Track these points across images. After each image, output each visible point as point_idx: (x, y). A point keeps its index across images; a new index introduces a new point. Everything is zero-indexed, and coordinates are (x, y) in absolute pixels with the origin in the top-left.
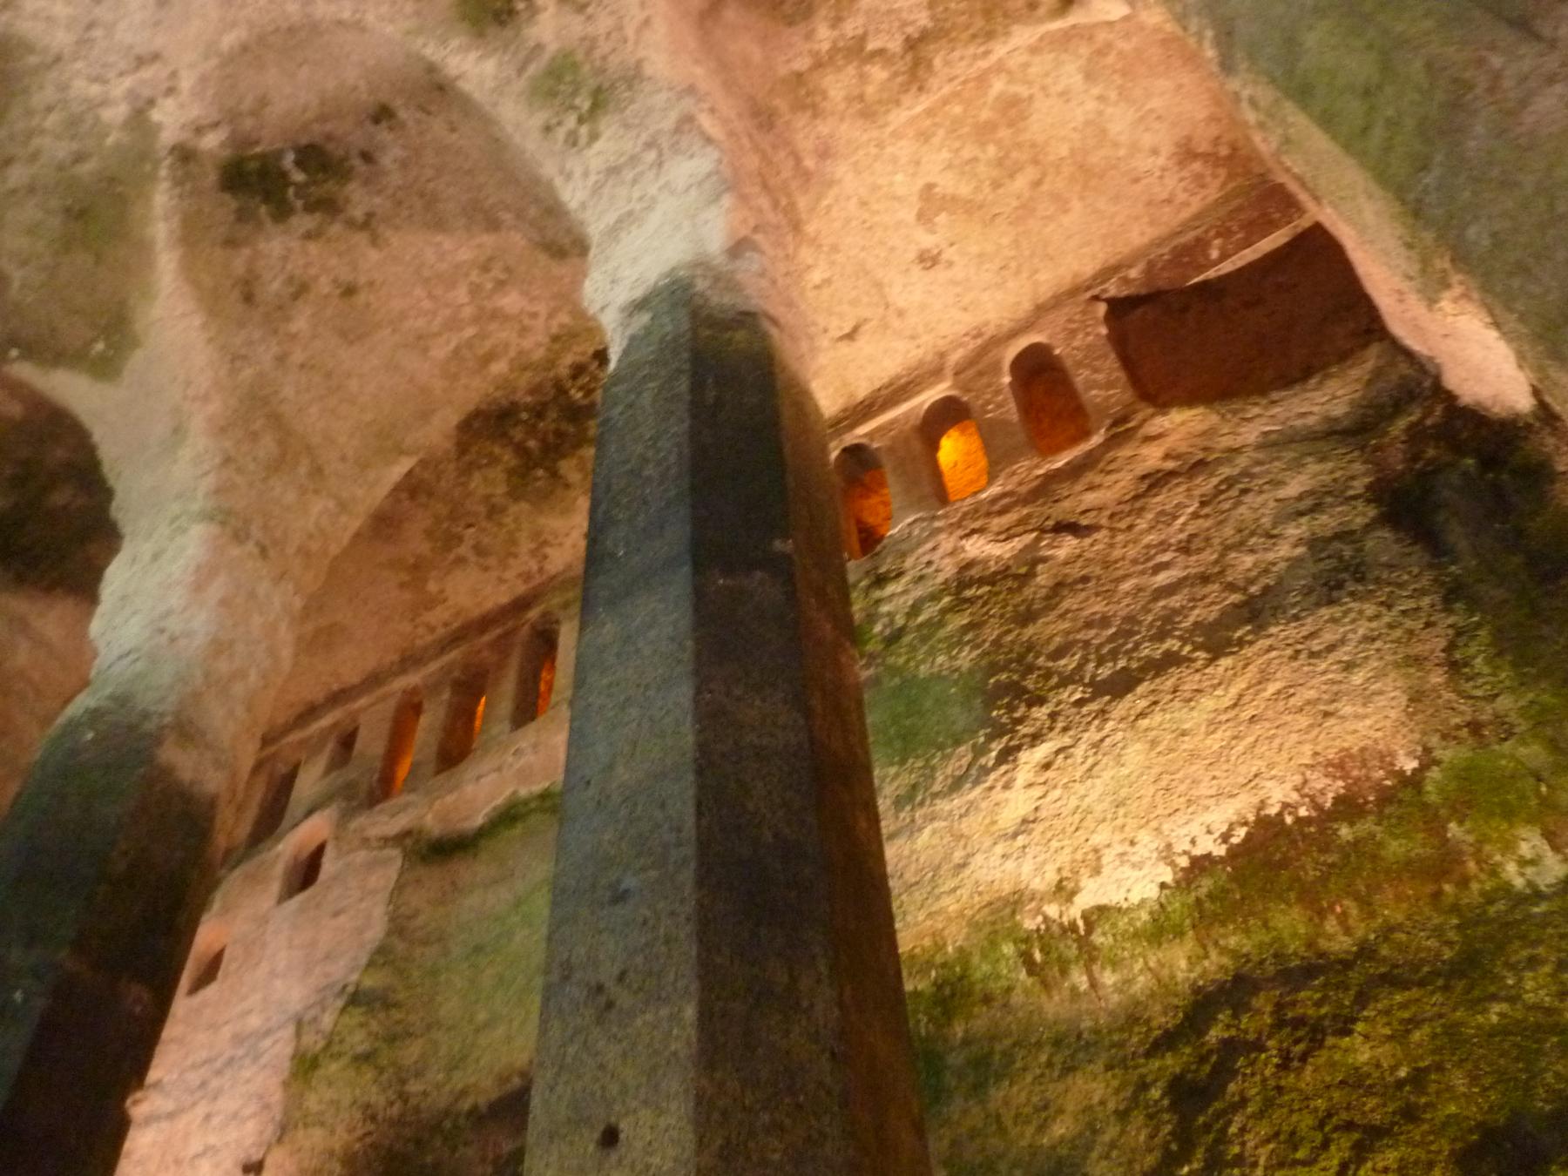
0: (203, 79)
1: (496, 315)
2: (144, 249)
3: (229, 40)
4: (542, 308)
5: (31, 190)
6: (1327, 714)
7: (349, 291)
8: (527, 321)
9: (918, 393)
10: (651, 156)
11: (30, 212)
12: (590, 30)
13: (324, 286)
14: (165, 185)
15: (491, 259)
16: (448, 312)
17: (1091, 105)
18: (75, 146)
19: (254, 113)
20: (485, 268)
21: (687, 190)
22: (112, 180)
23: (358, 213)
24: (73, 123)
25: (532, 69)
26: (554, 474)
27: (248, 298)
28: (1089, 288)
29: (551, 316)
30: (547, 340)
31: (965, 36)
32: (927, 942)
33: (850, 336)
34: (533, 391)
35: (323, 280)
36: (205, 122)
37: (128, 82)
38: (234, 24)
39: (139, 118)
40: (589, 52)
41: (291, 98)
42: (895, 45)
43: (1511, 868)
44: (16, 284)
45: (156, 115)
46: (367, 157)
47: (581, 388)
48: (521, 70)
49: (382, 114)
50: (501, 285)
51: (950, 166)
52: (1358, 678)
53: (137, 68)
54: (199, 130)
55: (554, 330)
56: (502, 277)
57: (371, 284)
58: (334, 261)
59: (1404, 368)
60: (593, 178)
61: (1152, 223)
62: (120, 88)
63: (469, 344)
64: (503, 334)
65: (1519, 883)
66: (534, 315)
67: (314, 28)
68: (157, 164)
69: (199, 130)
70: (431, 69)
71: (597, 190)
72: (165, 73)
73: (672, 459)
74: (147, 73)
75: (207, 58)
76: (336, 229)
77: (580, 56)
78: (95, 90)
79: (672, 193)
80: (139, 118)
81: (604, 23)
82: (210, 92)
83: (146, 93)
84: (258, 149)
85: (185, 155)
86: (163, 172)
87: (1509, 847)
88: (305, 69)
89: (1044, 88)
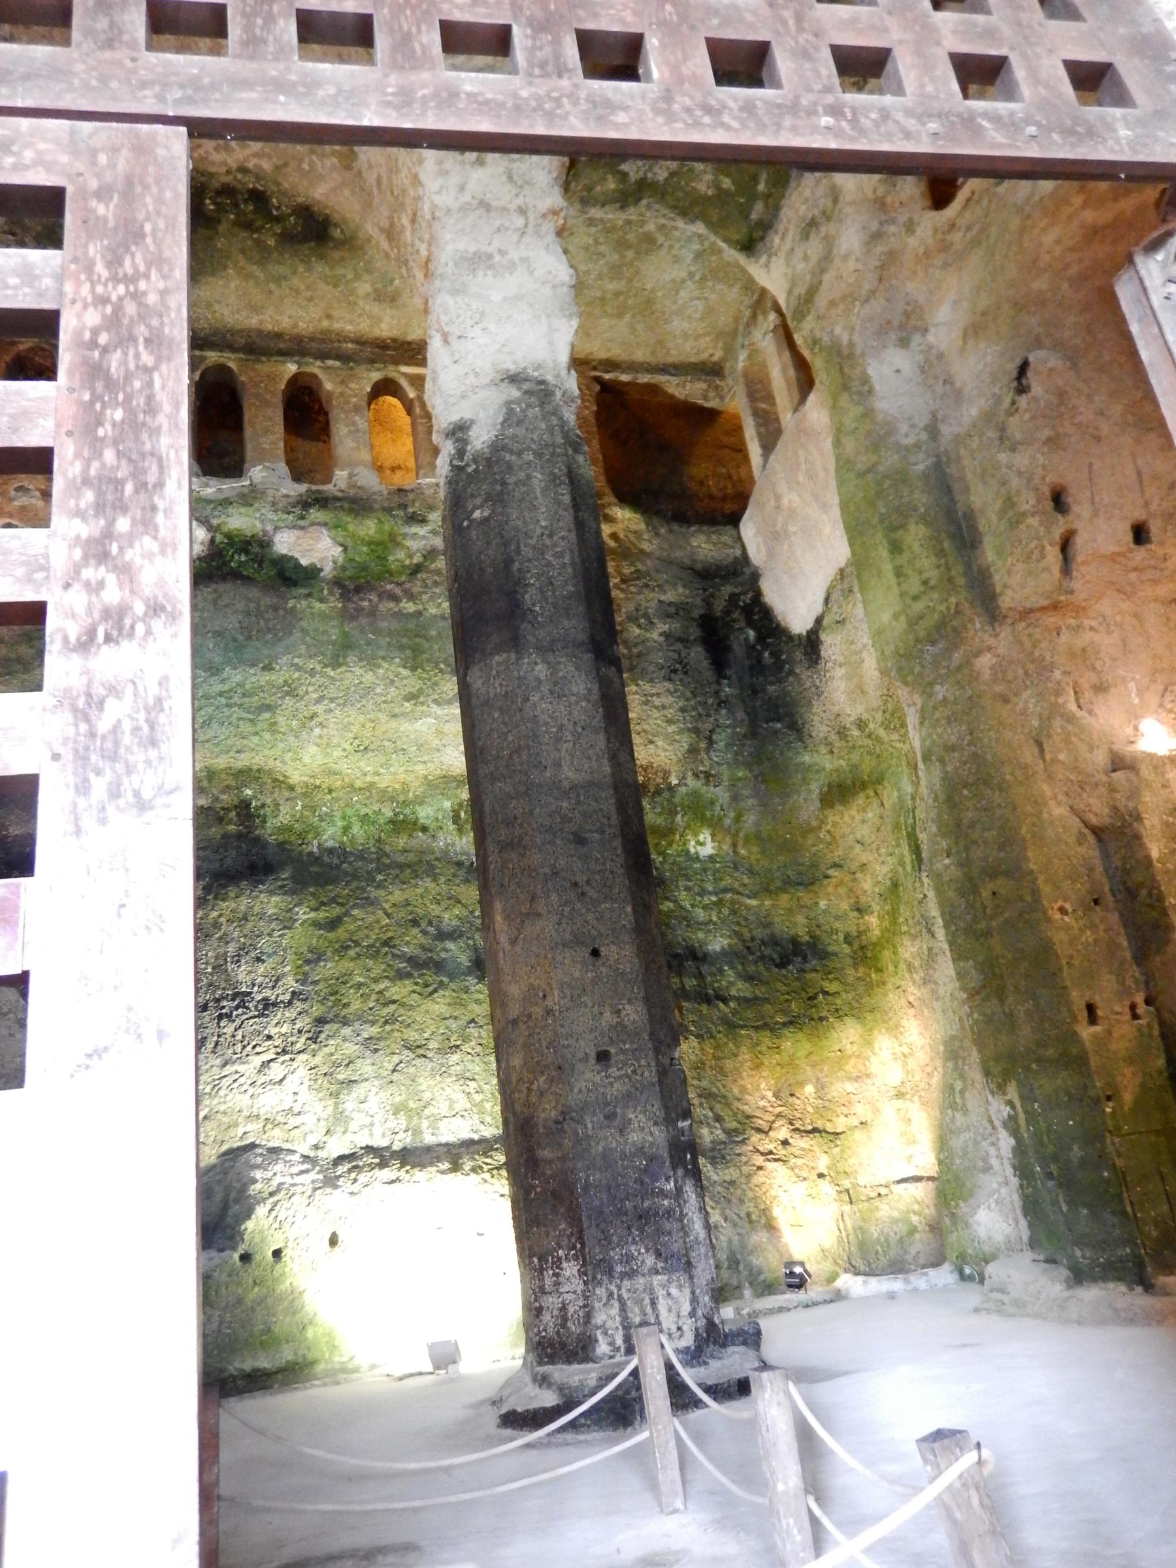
6: (651, 742)
10: (520, 222)
17: (684, 274)
21: (543, 283)
28: (595, 369)
31: (672, 203)
32: (397, 786)
42: (633, 177)
43: (693, 843)
47: (214, 203)
51: (587, 248)
52: (671, 729)
55: (250, 165)
59: (738, 552)
60: (466, 198)
61: (652, 353)
65: (692, 850)
71: (464, 209)
73: (567, 560)
79: (531, 273)
87: (696, 835)
89: (671, 247)
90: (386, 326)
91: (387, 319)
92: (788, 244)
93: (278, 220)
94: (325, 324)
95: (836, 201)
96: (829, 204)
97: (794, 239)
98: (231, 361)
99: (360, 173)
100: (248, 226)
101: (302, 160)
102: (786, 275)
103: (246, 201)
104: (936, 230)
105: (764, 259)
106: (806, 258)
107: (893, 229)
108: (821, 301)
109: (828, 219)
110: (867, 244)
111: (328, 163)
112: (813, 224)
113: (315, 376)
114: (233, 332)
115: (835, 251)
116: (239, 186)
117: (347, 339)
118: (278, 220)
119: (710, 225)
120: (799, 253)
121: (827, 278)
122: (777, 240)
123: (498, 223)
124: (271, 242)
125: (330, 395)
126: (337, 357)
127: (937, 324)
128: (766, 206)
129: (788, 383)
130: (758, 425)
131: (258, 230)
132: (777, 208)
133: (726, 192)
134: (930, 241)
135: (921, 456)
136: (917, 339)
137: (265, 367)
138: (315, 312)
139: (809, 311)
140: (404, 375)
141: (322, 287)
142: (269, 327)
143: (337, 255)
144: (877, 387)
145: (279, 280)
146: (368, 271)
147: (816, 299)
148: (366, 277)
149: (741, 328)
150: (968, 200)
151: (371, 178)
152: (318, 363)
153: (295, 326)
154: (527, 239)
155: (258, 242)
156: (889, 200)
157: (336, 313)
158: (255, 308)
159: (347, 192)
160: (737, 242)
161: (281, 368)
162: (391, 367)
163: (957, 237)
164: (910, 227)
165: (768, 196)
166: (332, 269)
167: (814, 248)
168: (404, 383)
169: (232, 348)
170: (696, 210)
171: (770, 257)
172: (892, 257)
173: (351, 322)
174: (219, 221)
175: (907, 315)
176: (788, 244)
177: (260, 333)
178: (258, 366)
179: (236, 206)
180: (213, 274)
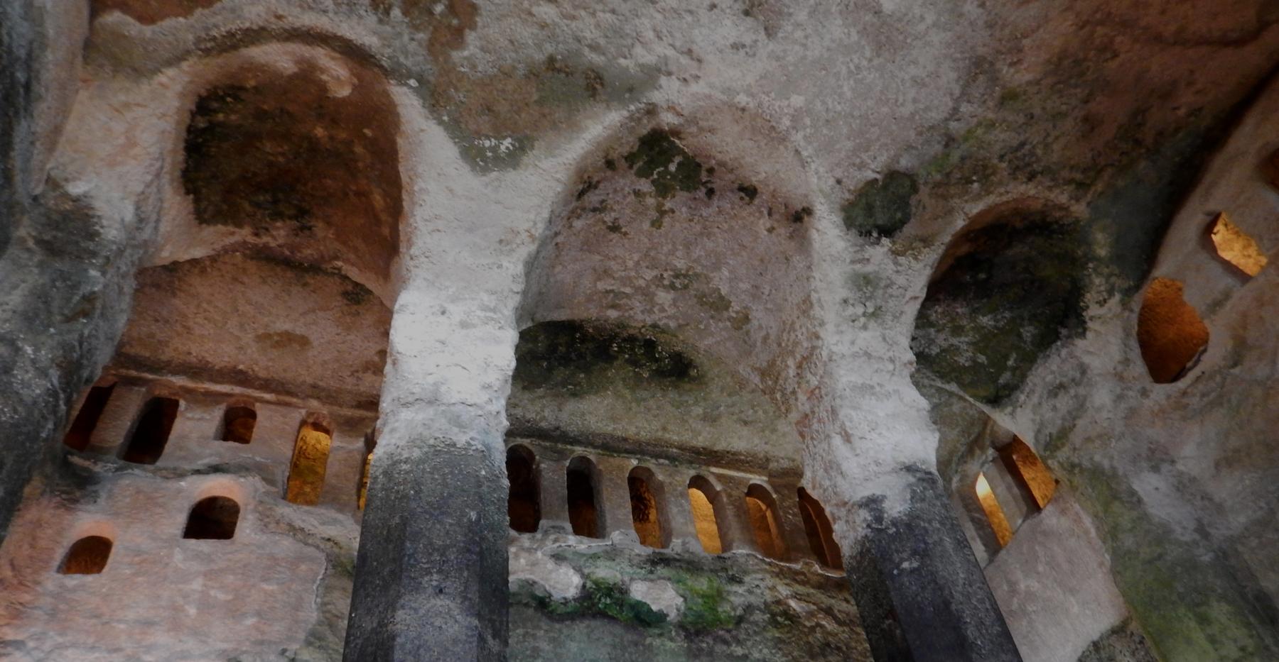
0: (709, 97)
1: (647, 294)
2: (574, 127)
3: (742, 99)
4: (671, 311)
5: (543, 26)
7: (615, 228)
8: (655, 310)
9: (751, 472)
11: (526, 33)
12: (894, 277)
13: (609, 218)
14: (625, 113)
15: (685, 276)
16: (633, 274)
18: (602, 42)
19: (701, 129)
20: (677, 276)
22: (599, 77)
23: (668, 205)
24: (618, 32)
25: (858, 267)
26: (550, 369)
27: (581, 194)
29: (668, 317)
30: (649, 321)
31: (937, 369)
33: (746, 423)
34: (595, 328)
35: (613, 214)
36: (678, 109)
37: (670, 52)
38: (752, 95)
39: (652, 74)
40: (887, 286)
41: (727, 144)
44: (466, 53)
45: (663, 80)
46: (710, 193)
48: (853, 262)
49: (749, 192)
50: (672, 287)
53: (682, 53)
54: (671, 108)
55: (661, 323)
56: (678, 285)
57: (625, 234)
58: (628, 211)
62: (662, 49)
63: (618, 295)
64: (637, 304)
66: (663, 310)
67: (783, 140)
68: (632, 100)
69: (671, 108)
70: (808, 211)
72: (695, 72)
74: (684, 60)
75: (723, 93)
76: (651, 201)
77: (882, 284)
78: (650, 35)
80: (652, 74)
81: (901, 280)
82: (701, 103)
83: (673, 68)
84: (677, 141)
85: (651, 111)
86: (632, 107)
88: (751, 144)
90: (703, 438)
91: (705, 434)
92: (1035, 399)
93: (657, 360)
94: (660, 434)
95: (1084, 372)
96: (1078, 375)
97: (1041, 397)
98: (592, 454)
99: (747, 333)
100: (634, 363)
101: (701, 322)
102: (1033, 421)
103: (640, 347)
104: (1169, 397)
105: (1009, 409)
106: (1054, 408)
107: (1130, 393)
108: (1076, 438)
109: (1078, 384)
110: (1115, 401)
111: (721, 325)
112: (1062, 386)
113: (648, 470)
114: (594, 434)
115: (1088, 404)
116: (640, 337)
117: (672, 446)
118: (657, 360)
119: (962, 385)
120: (1046, 407)
121: (1080, 423)
122: (1022, 397)
123: (876, 366)
124: (646, 375)
125: (661, 485)
126: (667, 457)
127: (1185, 458)
128: (1014, 375)
129: (1014, 498)
130: (977, 529)
131: (641, 366)
132: (1024, 377)
133: (982, 365)
134: (1164, 402)
135: (1202, 550)
136: (1165, 467)
137: (616, 461)
138: (656, 425)
139: (1063, 445)
140: (713, 473)
141: (669, 408)
142: (619, 433)
143: (687, 386)
144: (1145, 499)
145: (638, 401)
146: (705, 399)
147: (1071, 436)
148: (702, 404)
149: (955, 459)
150: (1198, 379)
151: (758, 336)
152: (654, 461)
153: (638, 434)
154: (895, 378)
155: (637, 375)
156: (1125, 374)
157: (670, 427)
158: (613, 419)
159: (729, 344)
160: (984, 397)
161: (626, 462)
162: (704, 468)
163: (1195, 402)
164: (1144, 393)
165: (1014, 369)
166: (680, 395)
167: (1064, 403)
168: (712, 480)
169: (595, 447)
170: (953, 375)
171: (1015, 408)
172: (1132, 413)
173: (678, 434)
174: (616, 358)
175: (1152, 451)
176: (1035, 399)
177: (612, 437)
178: (611, 460)
179: (632, 349)
180: (596, 393)
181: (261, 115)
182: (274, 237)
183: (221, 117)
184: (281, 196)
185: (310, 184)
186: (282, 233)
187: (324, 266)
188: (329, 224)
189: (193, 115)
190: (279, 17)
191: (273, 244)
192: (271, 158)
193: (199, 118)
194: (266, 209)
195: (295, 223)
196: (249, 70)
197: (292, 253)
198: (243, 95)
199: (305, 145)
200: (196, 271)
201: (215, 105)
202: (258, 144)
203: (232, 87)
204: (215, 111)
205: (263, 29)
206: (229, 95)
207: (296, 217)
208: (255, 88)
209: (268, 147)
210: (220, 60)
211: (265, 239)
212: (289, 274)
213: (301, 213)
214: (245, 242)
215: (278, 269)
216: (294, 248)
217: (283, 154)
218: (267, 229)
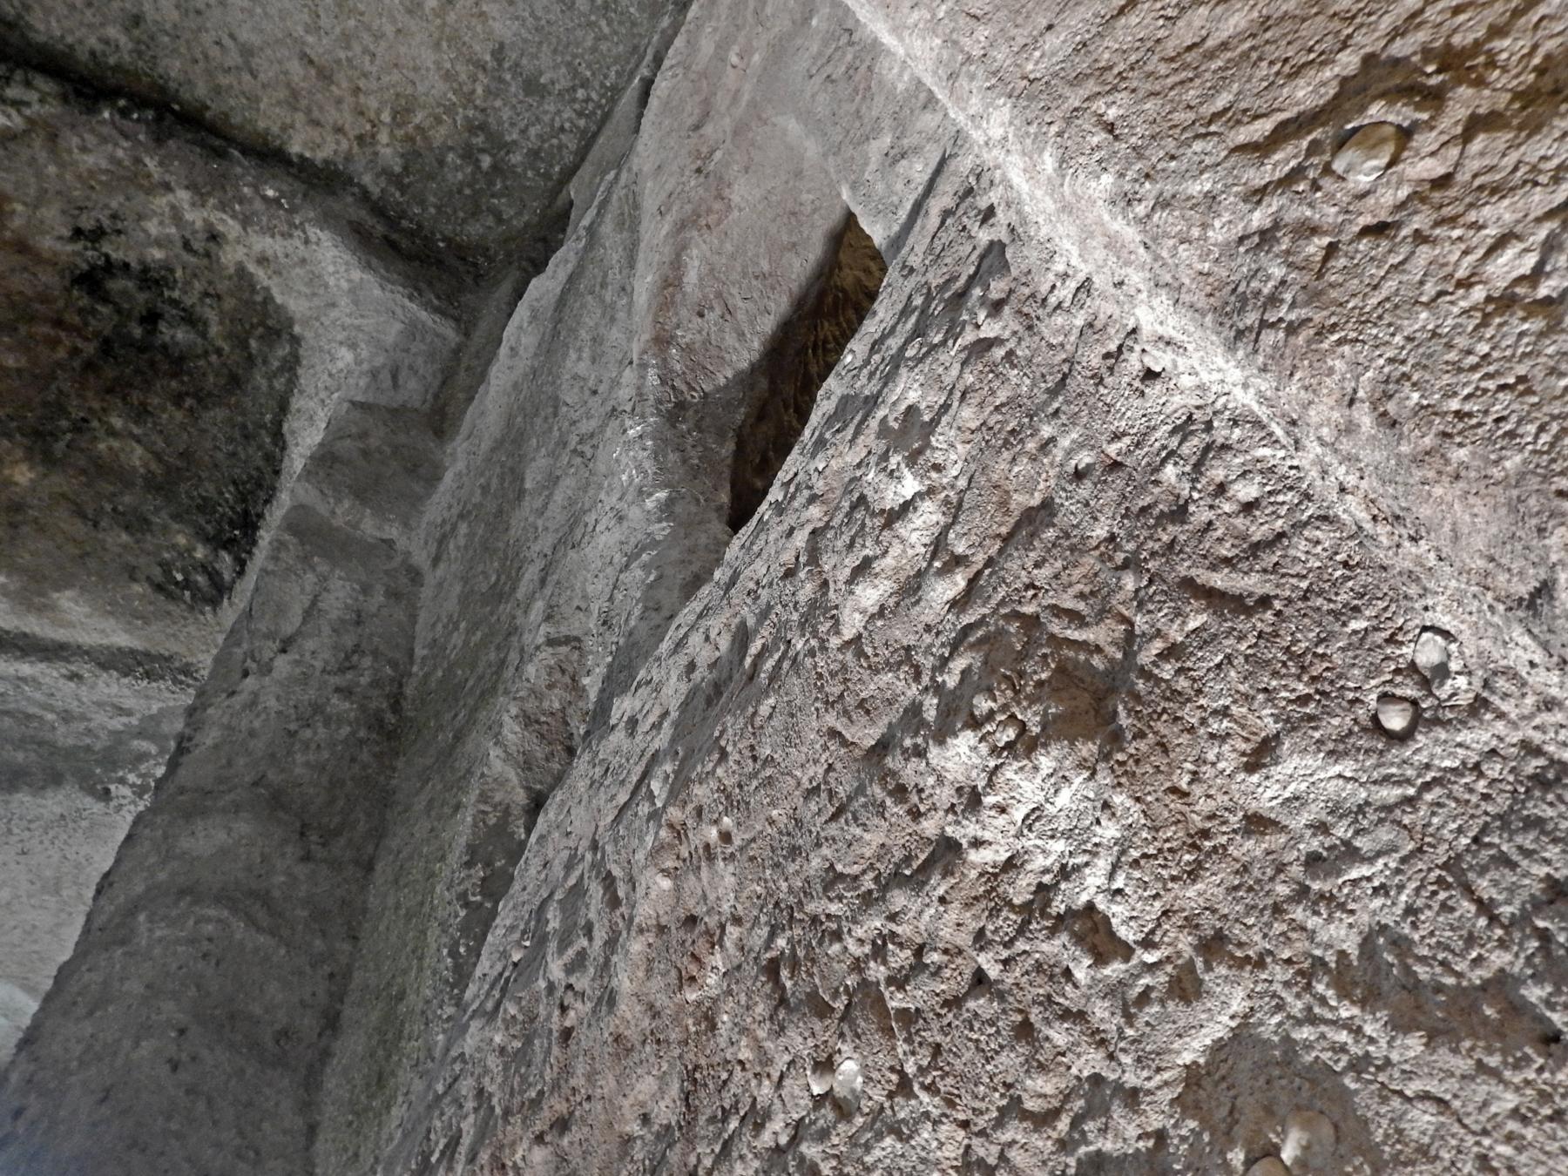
181: (137, 523)
182: (176, 216)
183: (200, 553)
184: (137, 332)
185: (61, 354)
186: (152, 227)
187: (52, 109)
188: (22, 247)
189: (230, 589)
190: (74, 677)
191: (183, 196)
192: (136, 431)
193: (227, 576)
194: (175, 303)
195: (115, 250)
196: (137, 615)
197: (138, 161)
198: (157, 572)
199: (59, 447)
200: (419, 117)
201: (201, 579)
202: (154, 466)
203: (170, 596)
204: (204, 568)
205: (104, 666)
206: (177, 583)
207: (109, 267)
208: (133, 579)
209: (136, 456)
210: (173, 647)
211: (195, 217)
212: (173, 68)
213: (92, 280)
214: (246, 222)
215: (202, 90)
216: (135, 179)
217: (112, 433)
218: (187, 245)
